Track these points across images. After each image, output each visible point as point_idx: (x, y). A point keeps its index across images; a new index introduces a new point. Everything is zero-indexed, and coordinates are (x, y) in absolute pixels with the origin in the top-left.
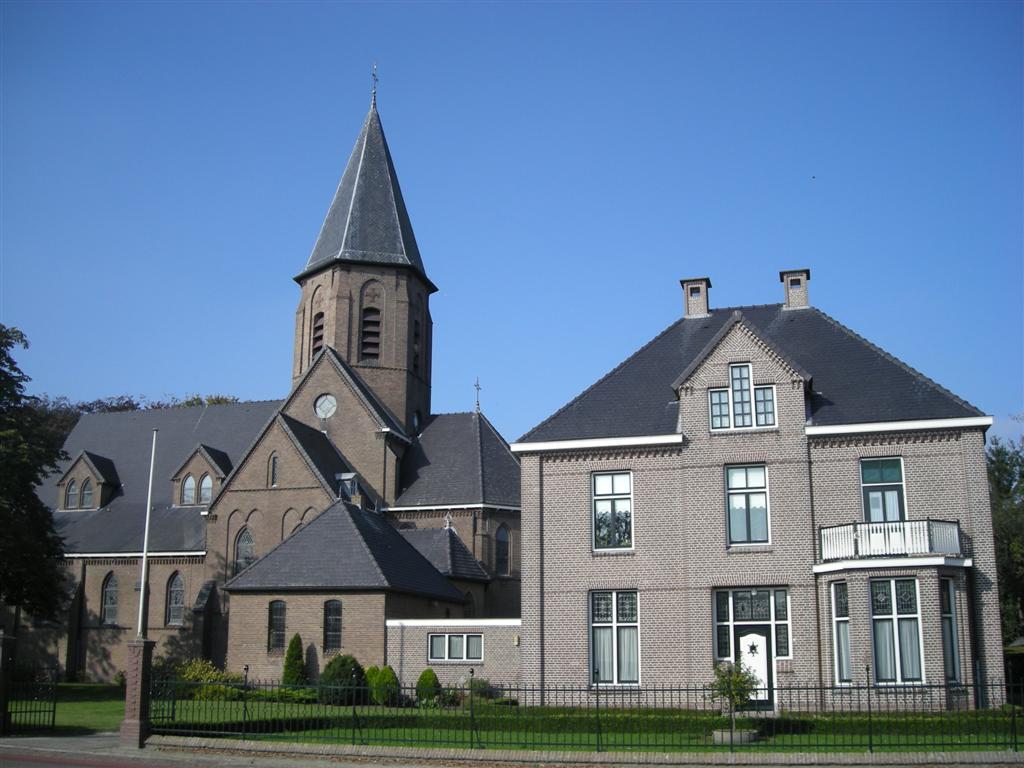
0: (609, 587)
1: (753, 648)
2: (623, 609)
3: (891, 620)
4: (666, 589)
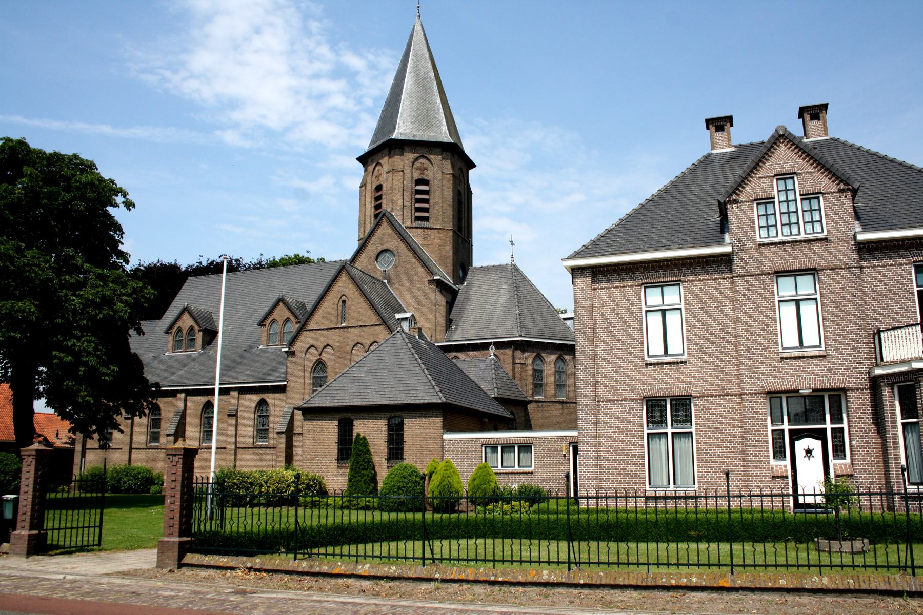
0: (663, 394)
1: (809, 452)
2: (653, 417)
4: (720, 396)
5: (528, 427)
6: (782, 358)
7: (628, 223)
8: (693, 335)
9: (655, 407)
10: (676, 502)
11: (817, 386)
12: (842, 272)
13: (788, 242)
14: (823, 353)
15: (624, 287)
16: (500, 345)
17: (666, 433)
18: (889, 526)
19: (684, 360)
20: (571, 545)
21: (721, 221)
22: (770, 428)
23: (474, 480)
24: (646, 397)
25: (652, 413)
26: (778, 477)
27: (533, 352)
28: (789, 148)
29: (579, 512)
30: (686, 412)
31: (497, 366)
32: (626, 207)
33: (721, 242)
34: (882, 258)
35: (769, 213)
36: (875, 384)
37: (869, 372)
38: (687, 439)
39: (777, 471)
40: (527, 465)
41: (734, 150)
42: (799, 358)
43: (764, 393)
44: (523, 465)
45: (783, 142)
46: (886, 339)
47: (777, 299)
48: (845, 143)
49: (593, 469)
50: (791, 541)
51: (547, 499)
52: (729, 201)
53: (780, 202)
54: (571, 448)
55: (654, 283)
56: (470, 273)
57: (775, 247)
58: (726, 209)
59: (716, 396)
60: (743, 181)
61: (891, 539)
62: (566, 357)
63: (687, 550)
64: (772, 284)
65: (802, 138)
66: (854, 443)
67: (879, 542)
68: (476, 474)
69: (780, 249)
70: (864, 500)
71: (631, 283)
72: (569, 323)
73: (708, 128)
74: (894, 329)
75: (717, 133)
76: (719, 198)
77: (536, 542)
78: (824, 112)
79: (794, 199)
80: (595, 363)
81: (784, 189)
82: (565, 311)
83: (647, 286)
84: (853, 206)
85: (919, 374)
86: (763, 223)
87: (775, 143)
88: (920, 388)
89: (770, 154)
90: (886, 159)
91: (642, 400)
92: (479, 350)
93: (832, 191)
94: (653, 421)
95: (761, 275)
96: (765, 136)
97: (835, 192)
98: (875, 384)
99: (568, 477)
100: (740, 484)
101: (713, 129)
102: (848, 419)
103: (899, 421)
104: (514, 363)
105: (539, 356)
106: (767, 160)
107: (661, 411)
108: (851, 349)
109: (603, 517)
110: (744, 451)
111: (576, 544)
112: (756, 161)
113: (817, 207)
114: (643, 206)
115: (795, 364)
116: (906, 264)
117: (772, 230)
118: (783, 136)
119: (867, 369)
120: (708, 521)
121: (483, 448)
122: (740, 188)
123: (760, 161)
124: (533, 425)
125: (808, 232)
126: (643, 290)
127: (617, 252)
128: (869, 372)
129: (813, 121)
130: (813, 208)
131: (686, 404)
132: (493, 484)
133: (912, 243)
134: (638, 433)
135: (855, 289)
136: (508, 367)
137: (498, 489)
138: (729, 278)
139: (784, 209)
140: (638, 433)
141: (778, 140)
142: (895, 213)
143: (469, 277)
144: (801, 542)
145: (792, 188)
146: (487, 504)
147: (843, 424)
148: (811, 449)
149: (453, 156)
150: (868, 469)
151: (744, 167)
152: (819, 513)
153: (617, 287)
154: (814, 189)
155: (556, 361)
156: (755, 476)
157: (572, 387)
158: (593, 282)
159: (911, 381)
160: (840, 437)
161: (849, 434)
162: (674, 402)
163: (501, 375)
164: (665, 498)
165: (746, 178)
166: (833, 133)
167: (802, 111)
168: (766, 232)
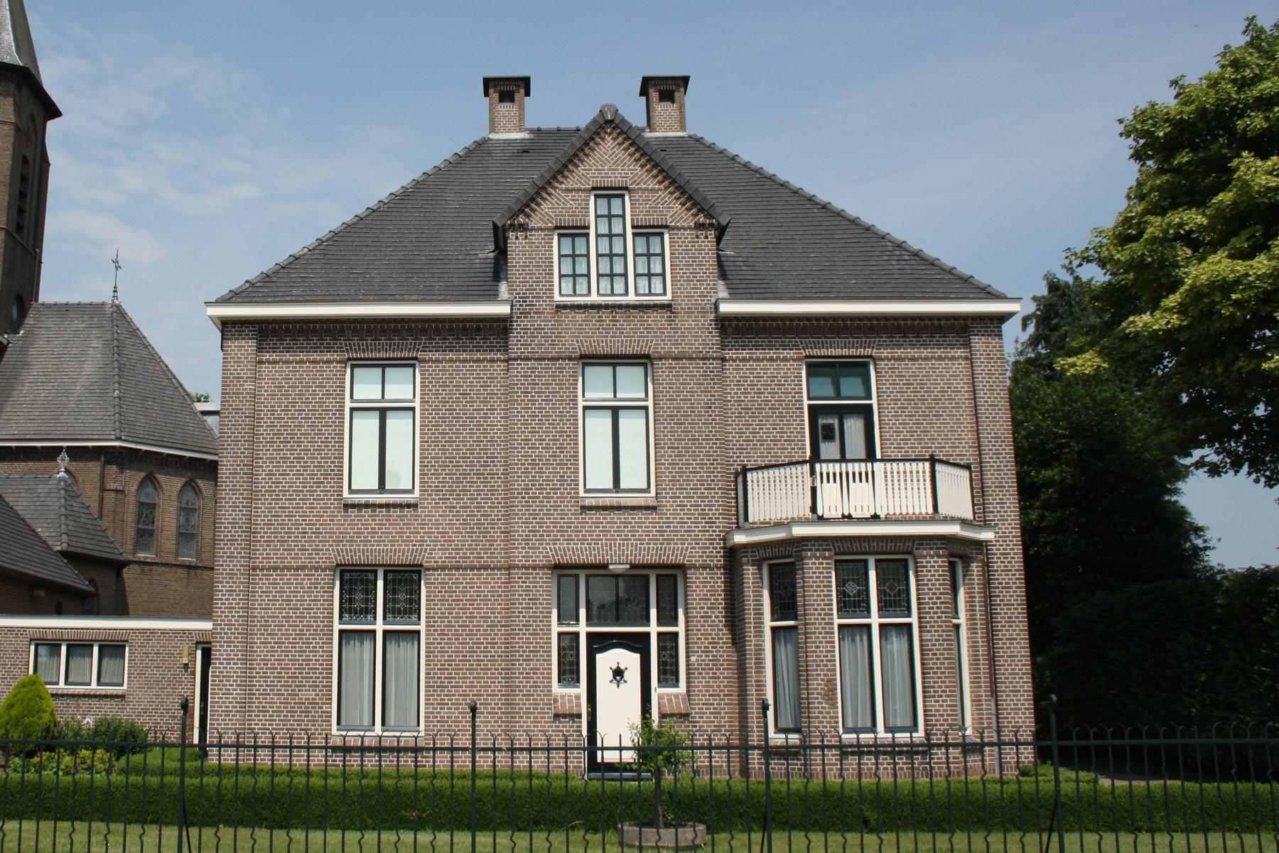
0: (372, 560)
1: (618, 673)
2: (394, 601)
3: (869, 626)
4: (472, 568)
5: (121, 610)
6: (583, 508)
7: (332, 248)
8: (432, 458)
9: (356, 584)
10: (398, 757)
11: (639, 559)
12: (691, 366)
13: (607, 307)
14: (651, 503)
15: (315, 362)
16: (75, 454)
17: (374, 632)
18: (740, 802)
19: (412, 501)
20: (185, 833)
21: (496, 258)
22: (556, 629)
23: (10, 706)
24: (341, 565)
25: (351, 594)
26: (565, 716)
27: (141, 470)
28: (620, 144)
29: (202, 772)
30: (411, 594)
31: (71, 490)
32: (333, 217)
33: (492, 297)
34: (757, 347)
35: (577, 252)
36: (733, 556)
37: (724, 539)
38: (409, 644)
39: (563, 704)
40: (115, 681)
41: (527, 136)
42: (612, 508)
43: (549, 568)
44: (107, 681)
45: (610, 134)
46: (755, 483)
47: (581, 404)
48: (711, 147)
49: (237, 692)
50: (579, 829)
51: (144, 747)
52: (512, 225)
53: (598, 236)
54: (199, 653)
55: (369, 359)
56: (31, 314)
57: (584, 313)
58: (506, 239)
59: (466, 569)
60: (538, 193)
61: (742, 825)
62: (201, 483)
63: (395, 845)
64: (575, 376)
65: (643, 130)
66: (693, 659)
67: (722, 830)
68: (15, 695)
69: (592, 317)
70: (702, 757)
71: (327, 357)
72: (210, 420)
73: (486, 94)
74: (768, 467)
75: (502, 104)
76: (494, 219)
77: (120, 827)
78: (682, 89)
79: (621, 232)
80: (252, 496)
81: (606, 213)
82: (206, 399)
83: (356, 364)
84: (718, 254)
85: (803, 546)
86: (567, 269)
87: (597, 133)
88: (803, 569)
89: (587, 151)
90: (773, 181)
91: (333, 569)
92: (39, 460)
93: (685, 225)
94: (350, 608)
95: (557, 359)
96: (581, 119)
97: (690, 228)
98: (733, 556)
99: (186, 706)
100: (499, 726)
101: (496, 96)
102: (687, 617)
103: (768, 623)
104: (103, 489)
105: (150, 479)
106: (582, 161)
107: (367, 592)
108: (698, 497)
109: (246, 782)
110: (508, 669)
111: (194, 832)
112: (564, 160)
113: (658, 251)
114: (361, 219)
115: (604, 518)
116: (794, 360)
117: (582, 284)
118: (611, 122)
119: (723, 534)
120: (437, 792)
121: (32, 648)
122: (533, 205)
123: (570, 161)
124: (130, 607)
125: (641, 291)
126: (349, 370)
127: (308, 298)
128: (724, 539)
129: (663, 104)
130: (651, 252)
131: (412, 581)
132: (46, 716)
133: (805, 326)
134: (321, 630)
135: (711, 396)
136: (91, 495)
137: (55, 725)
138: (501, 361)
139: (604, 249)
140: (321, 630)
141: (604, 128)
142: (782, 273)
143: (29, 321)
144: (596, 831)
145: (621, 213)
146: (30, 754)
147: (677, 626)
148: (622, 667)
149: (20, 91)
150: (713, 704)
151: (543, 169)
152: (627, 780)
153: (301, 362)
154: (655, 219)
155: (182, 491)
156: (524, 713)
157: (208, 539)
158: (260, 349)
159: (790, 556)
160: (671, 649)
161: (687, 644)
162: (390, 576)
163: (75, 509)
164: (363, 749)
165: (544, 189)
166: (695, 128)
167: (647, 85)
168: (571, 285)
